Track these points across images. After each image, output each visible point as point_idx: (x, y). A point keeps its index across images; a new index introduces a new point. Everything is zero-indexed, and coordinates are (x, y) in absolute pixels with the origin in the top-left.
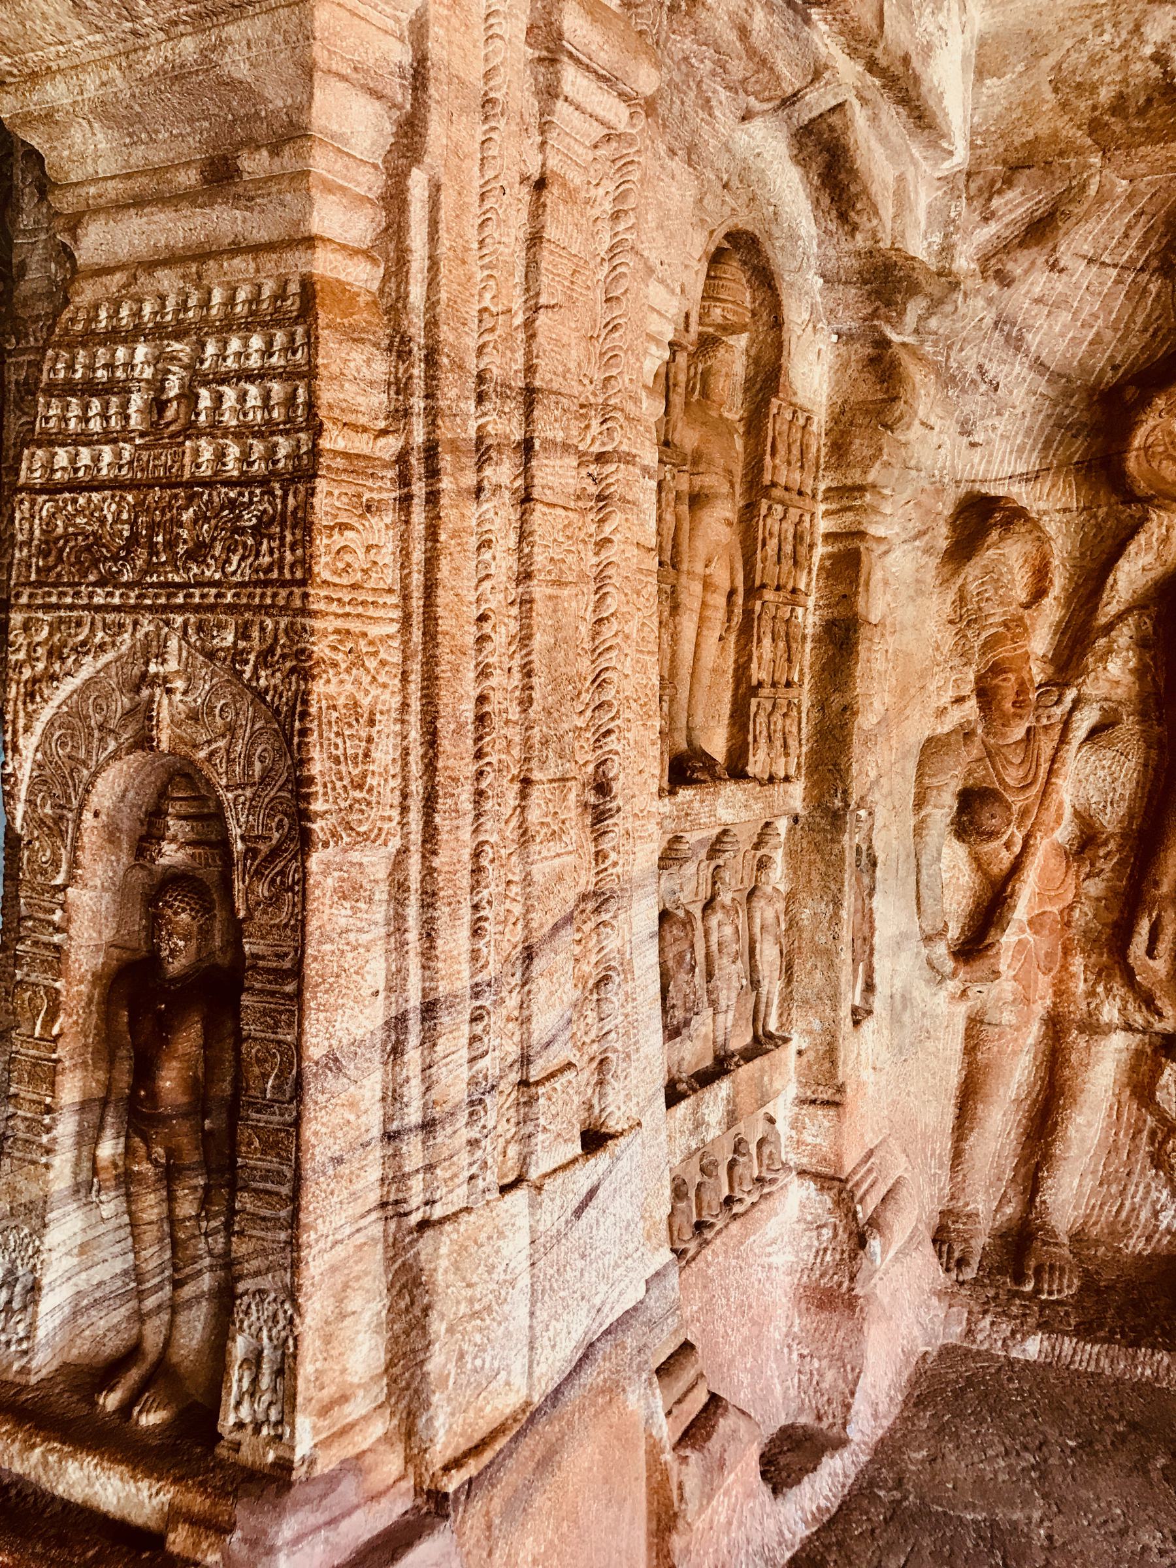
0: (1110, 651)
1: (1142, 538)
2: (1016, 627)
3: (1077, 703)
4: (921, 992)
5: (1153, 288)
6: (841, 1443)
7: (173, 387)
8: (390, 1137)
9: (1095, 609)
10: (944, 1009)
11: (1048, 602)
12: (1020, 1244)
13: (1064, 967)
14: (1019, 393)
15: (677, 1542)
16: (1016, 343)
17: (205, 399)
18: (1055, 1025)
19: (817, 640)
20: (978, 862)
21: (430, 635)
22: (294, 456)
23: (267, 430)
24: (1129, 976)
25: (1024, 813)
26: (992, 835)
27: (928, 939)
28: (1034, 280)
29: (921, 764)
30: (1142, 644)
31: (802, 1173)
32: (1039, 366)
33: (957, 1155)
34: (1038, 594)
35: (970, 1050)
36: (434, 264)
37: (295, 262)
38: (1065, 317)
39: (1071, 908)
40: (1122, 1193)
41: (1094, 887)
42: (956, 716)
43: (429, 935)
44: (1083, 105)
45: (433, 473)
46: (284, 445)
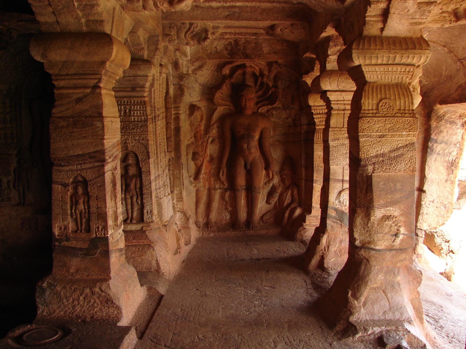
0: (213, 129)
1: (217, 111)
2: (199, 125)
3: (209, 137)
4: (189, 186)
5: (216, 74)
6: (190, 244)
7: (127, 111)
8: (156, 189)
9: (210, 122)
10: (193, 189)
11: (203, 121)
12: (207, 225)
13: (210, 180)
14: (197, 88)
15: (180, 242)
16: (197, 81)
17: (132, 112)
18: (209, 190)
19: (174, 130)
20: (196, 164)
21: (156, 136)
22: (144, 119)
23: (140, 116)
24: (220, 179)
25: (202, 156)
26: (198, 160)
27: (190, 177)
28: (199, 73)
29: (187, 149)
30: (218, 127)
31: (178, 211)
32: (200, 84)
33: (196, 212)
34: (202, 120)
35: (197, 195)
36: (154, 98)
37: (143, 99)
38: (204, 77)
39: (210, 171)
40: (221, 215)
41: (214, 166)
42: (191, 140)
43: (158, 168)
44: (206, 53)
45: (155, 119)
46: (143, 118)
